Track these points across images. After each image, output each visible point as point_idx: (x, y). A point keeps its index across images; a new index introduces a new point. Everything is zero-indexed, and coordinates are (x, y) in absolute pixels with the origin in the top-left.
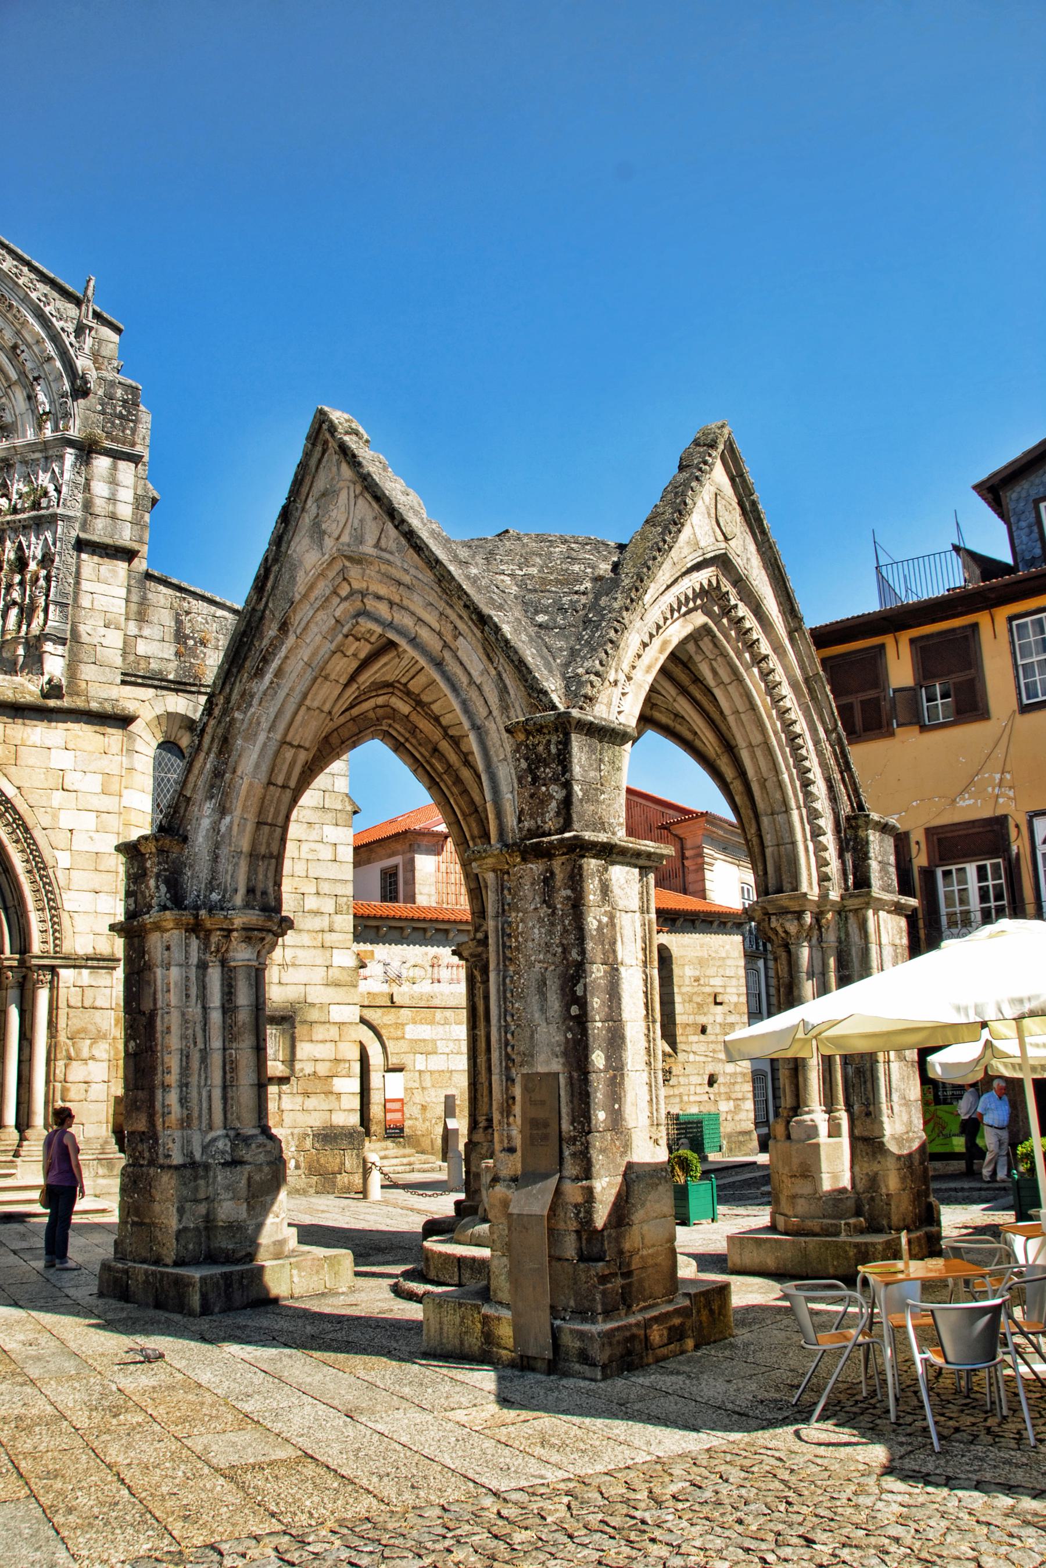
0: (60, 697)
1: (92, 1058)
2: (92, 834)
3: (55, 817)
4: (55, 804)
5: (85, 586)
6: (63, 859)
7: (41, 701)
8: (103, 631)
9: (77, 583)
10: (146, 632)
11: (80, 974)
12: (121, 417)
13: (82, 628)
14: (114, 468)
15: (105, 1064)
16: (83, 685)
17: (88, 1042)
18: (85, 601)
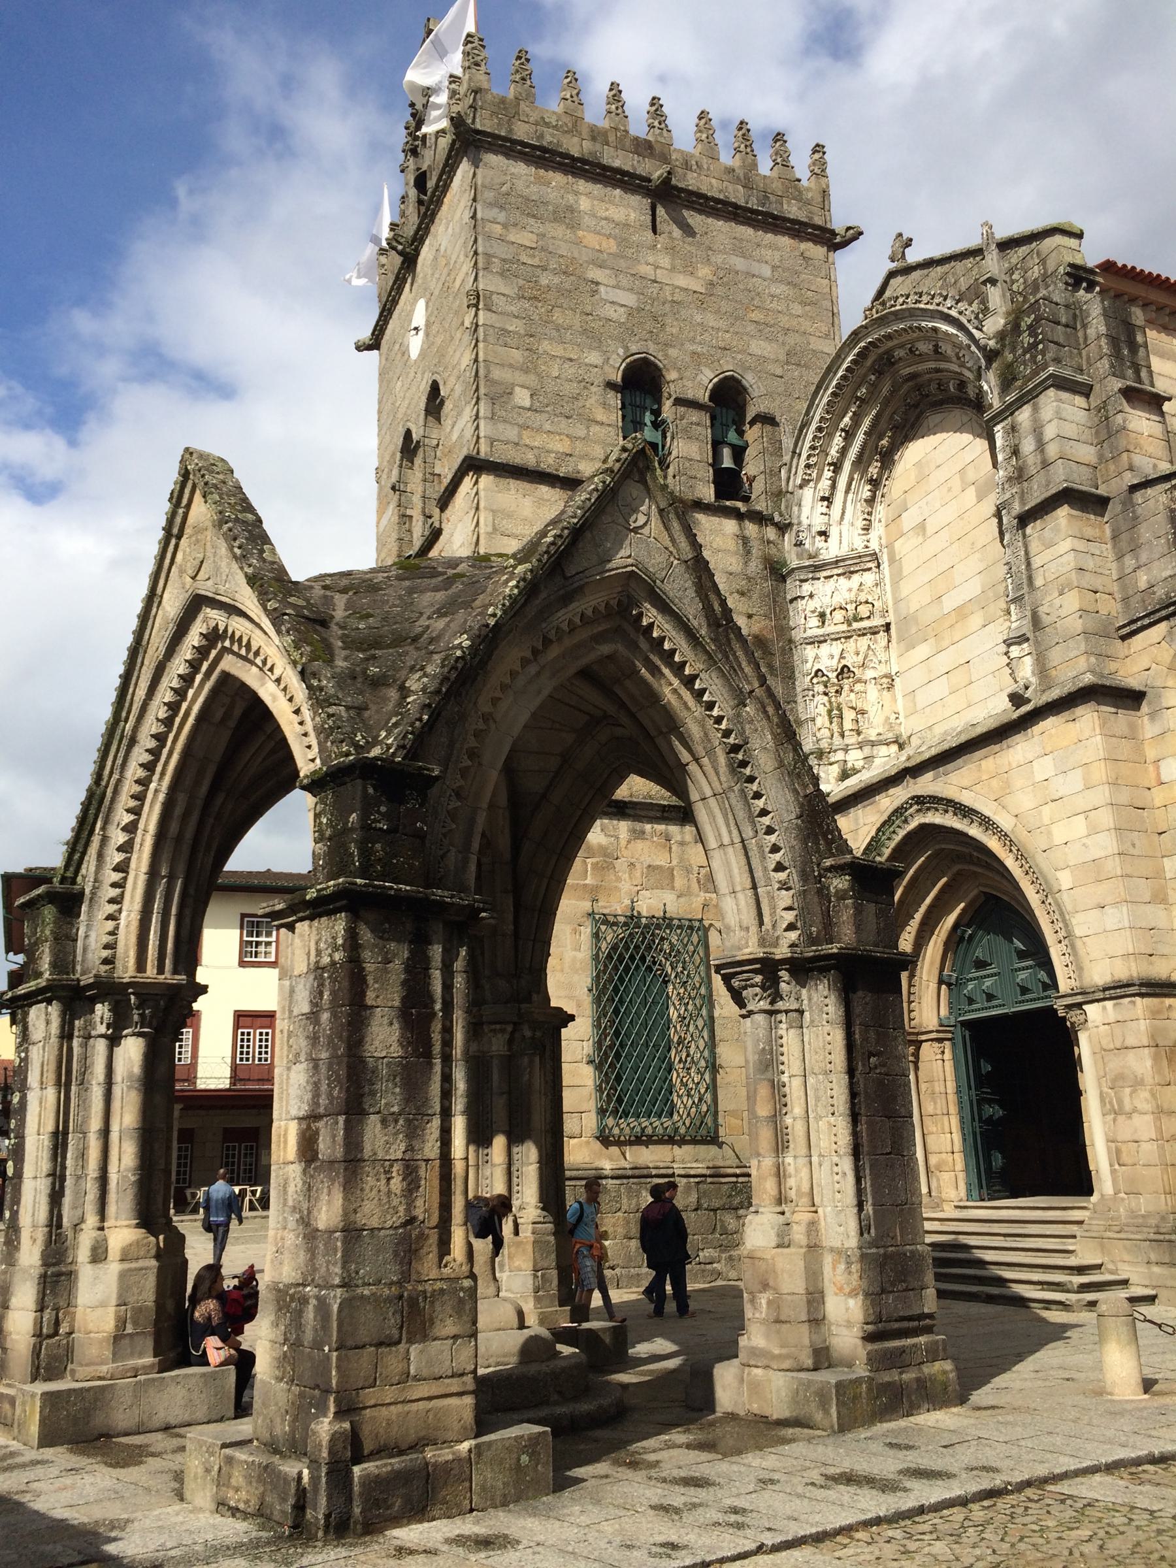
0: (1028, 701)
1: (1135, 1110)
2: (1084, 840)
3: (1049, 833)
4: (1046, 821)
5: (1036, 562)
6: (1064, 880)
7: (1015, 715)
8: (1057, 602)
9: (1029, 564)
10: (1144, 558)
11: (1104, 1008)
12: (1034, 346)
13: (1042, 610)
14: (1036, 409)
15: (1149, 1118)
16: (1053, 673)
17: (1128, 1090)
18: (1039, 582)
